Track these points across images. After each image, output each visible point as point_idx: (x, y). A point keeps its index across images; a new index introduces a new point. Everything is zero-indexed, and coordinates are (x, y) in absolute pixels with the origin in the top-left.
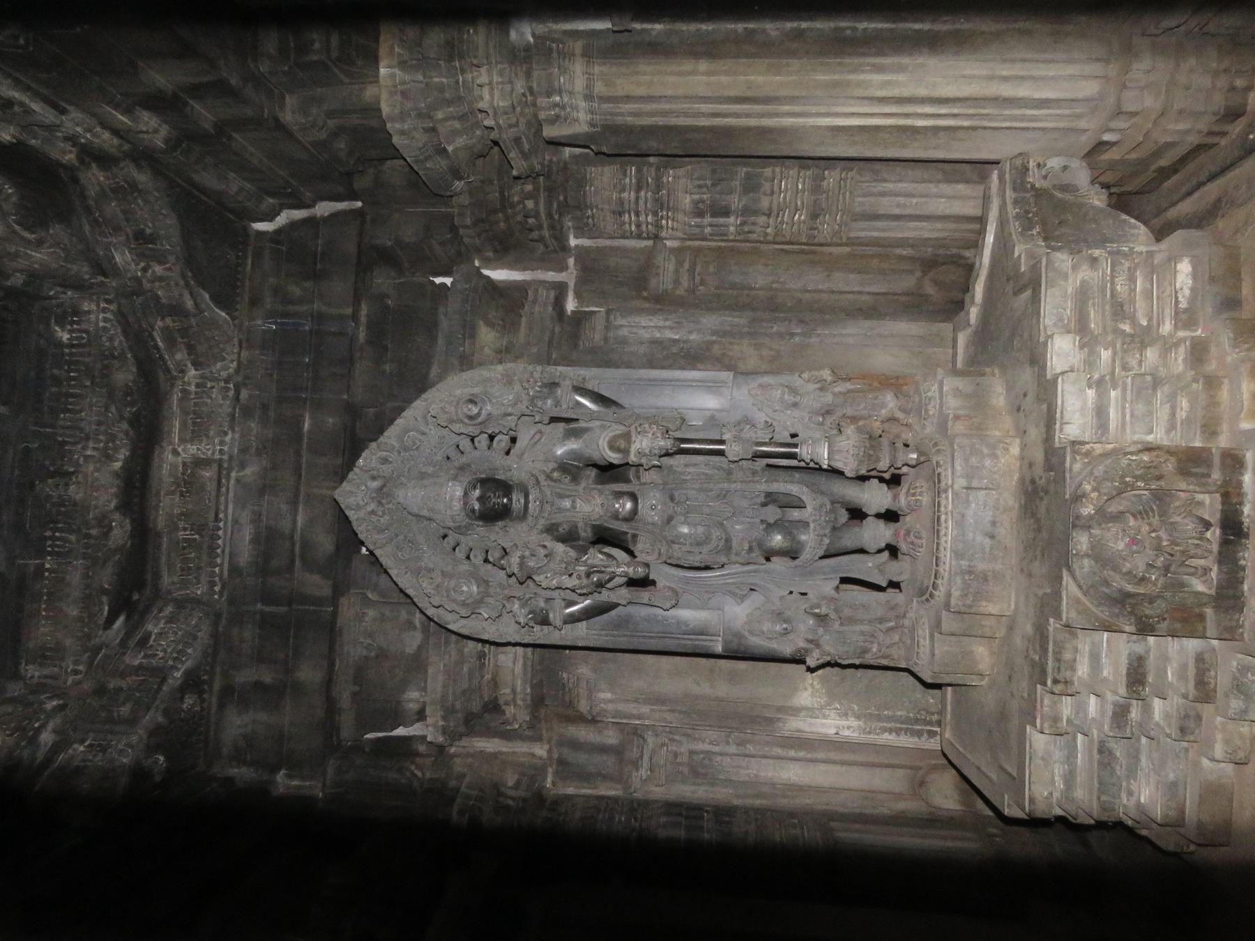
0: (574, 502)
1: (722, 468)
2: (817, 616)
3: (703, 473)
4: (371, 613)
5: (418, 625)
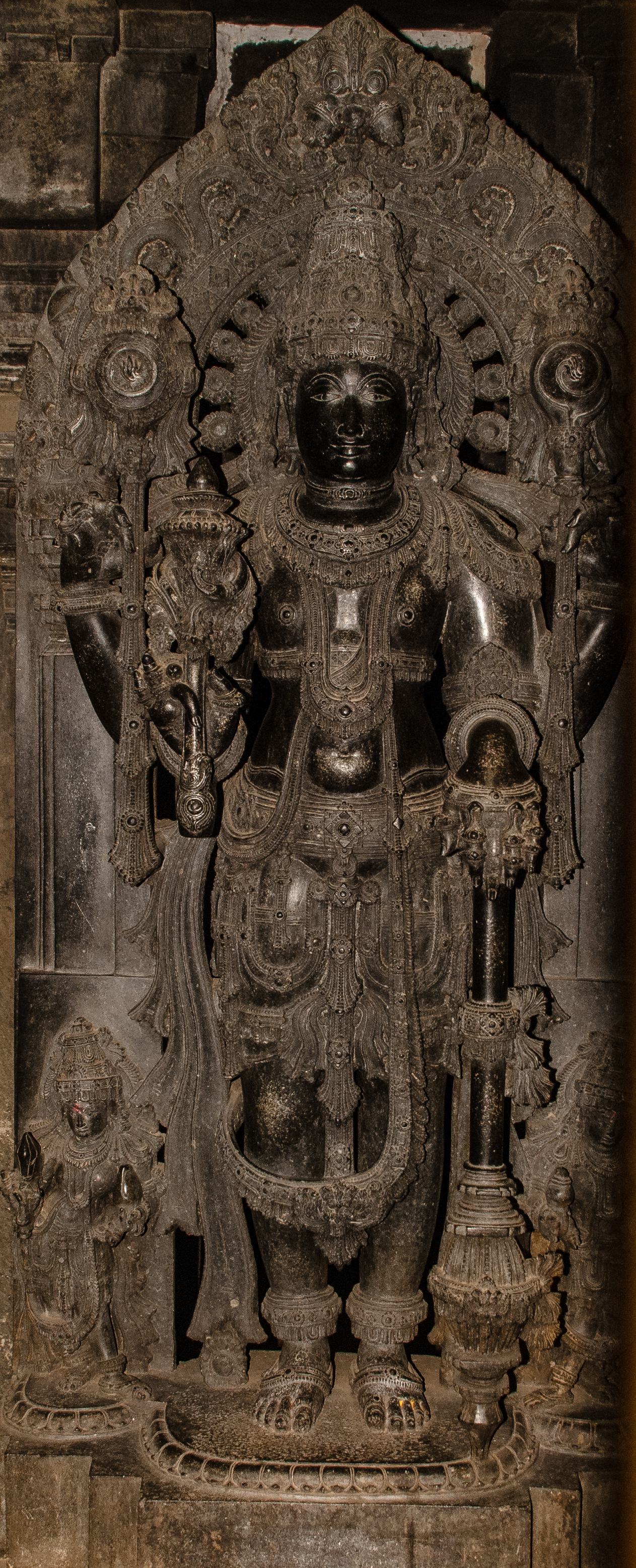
0: (352, 636)
1: (443, 978)
2: (115, 1188)
3: (427, 940)
4: (69, 70)
5: (46, 191)
